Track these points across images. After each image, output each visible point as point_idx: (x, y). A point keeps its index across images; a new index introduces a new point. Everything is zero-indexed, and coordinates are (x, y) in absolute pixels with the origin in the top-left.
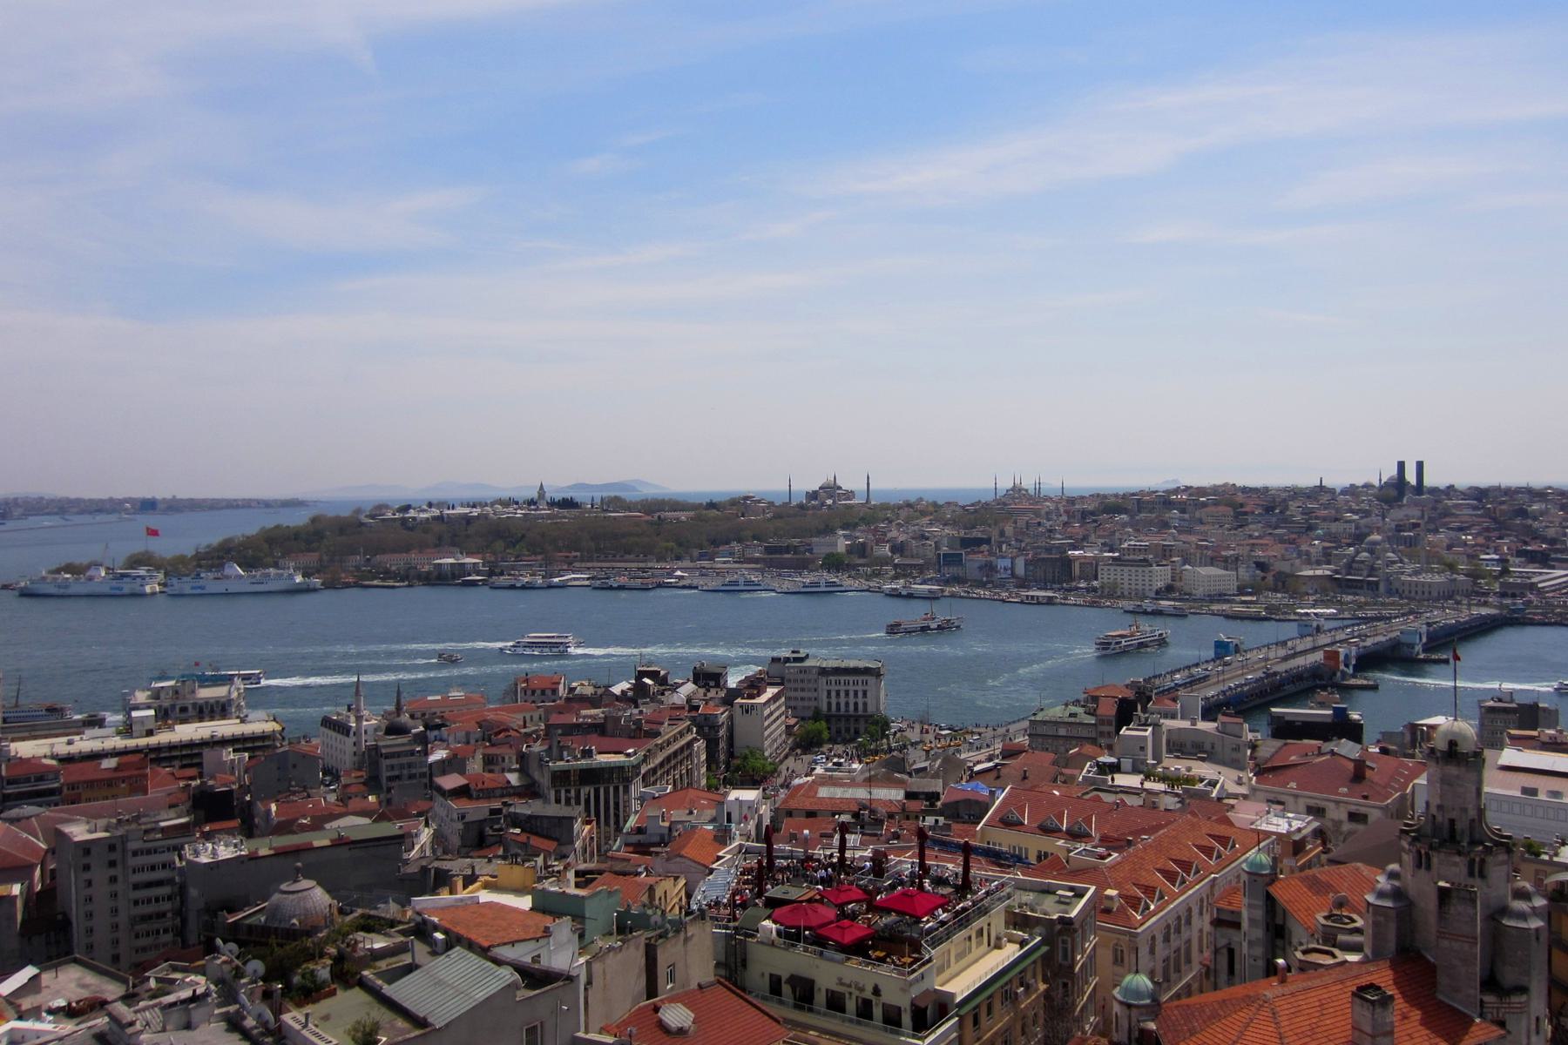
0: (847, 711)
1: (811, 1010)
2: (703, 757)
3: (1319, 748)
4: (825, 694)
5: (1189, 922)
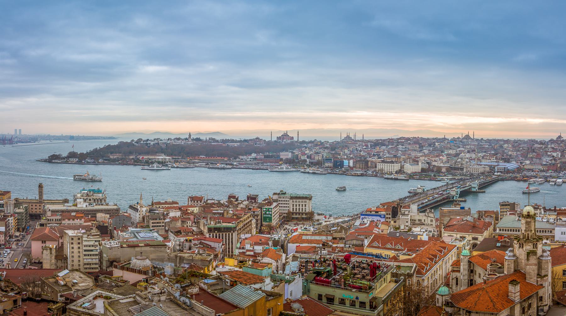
1: (333, 304)
2: (255, 225)
4: (292, 205)
5: (437, 272)
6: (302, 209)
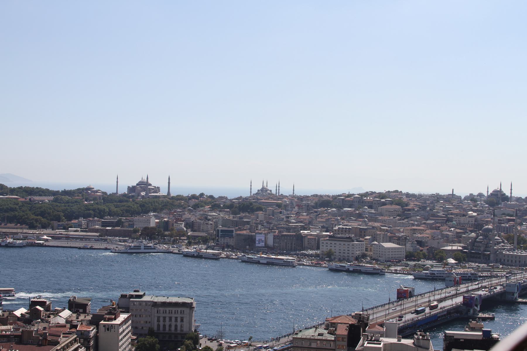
0: (170, 330)
4: (156, 319)
6: (176, 326)
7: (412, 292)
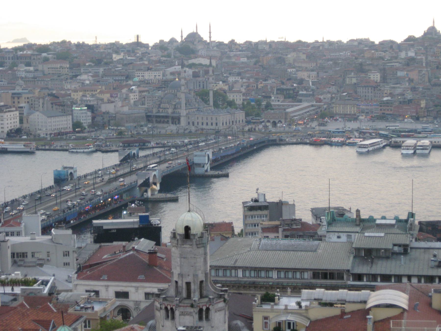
3: (124, 247)
7: (73, 172)
